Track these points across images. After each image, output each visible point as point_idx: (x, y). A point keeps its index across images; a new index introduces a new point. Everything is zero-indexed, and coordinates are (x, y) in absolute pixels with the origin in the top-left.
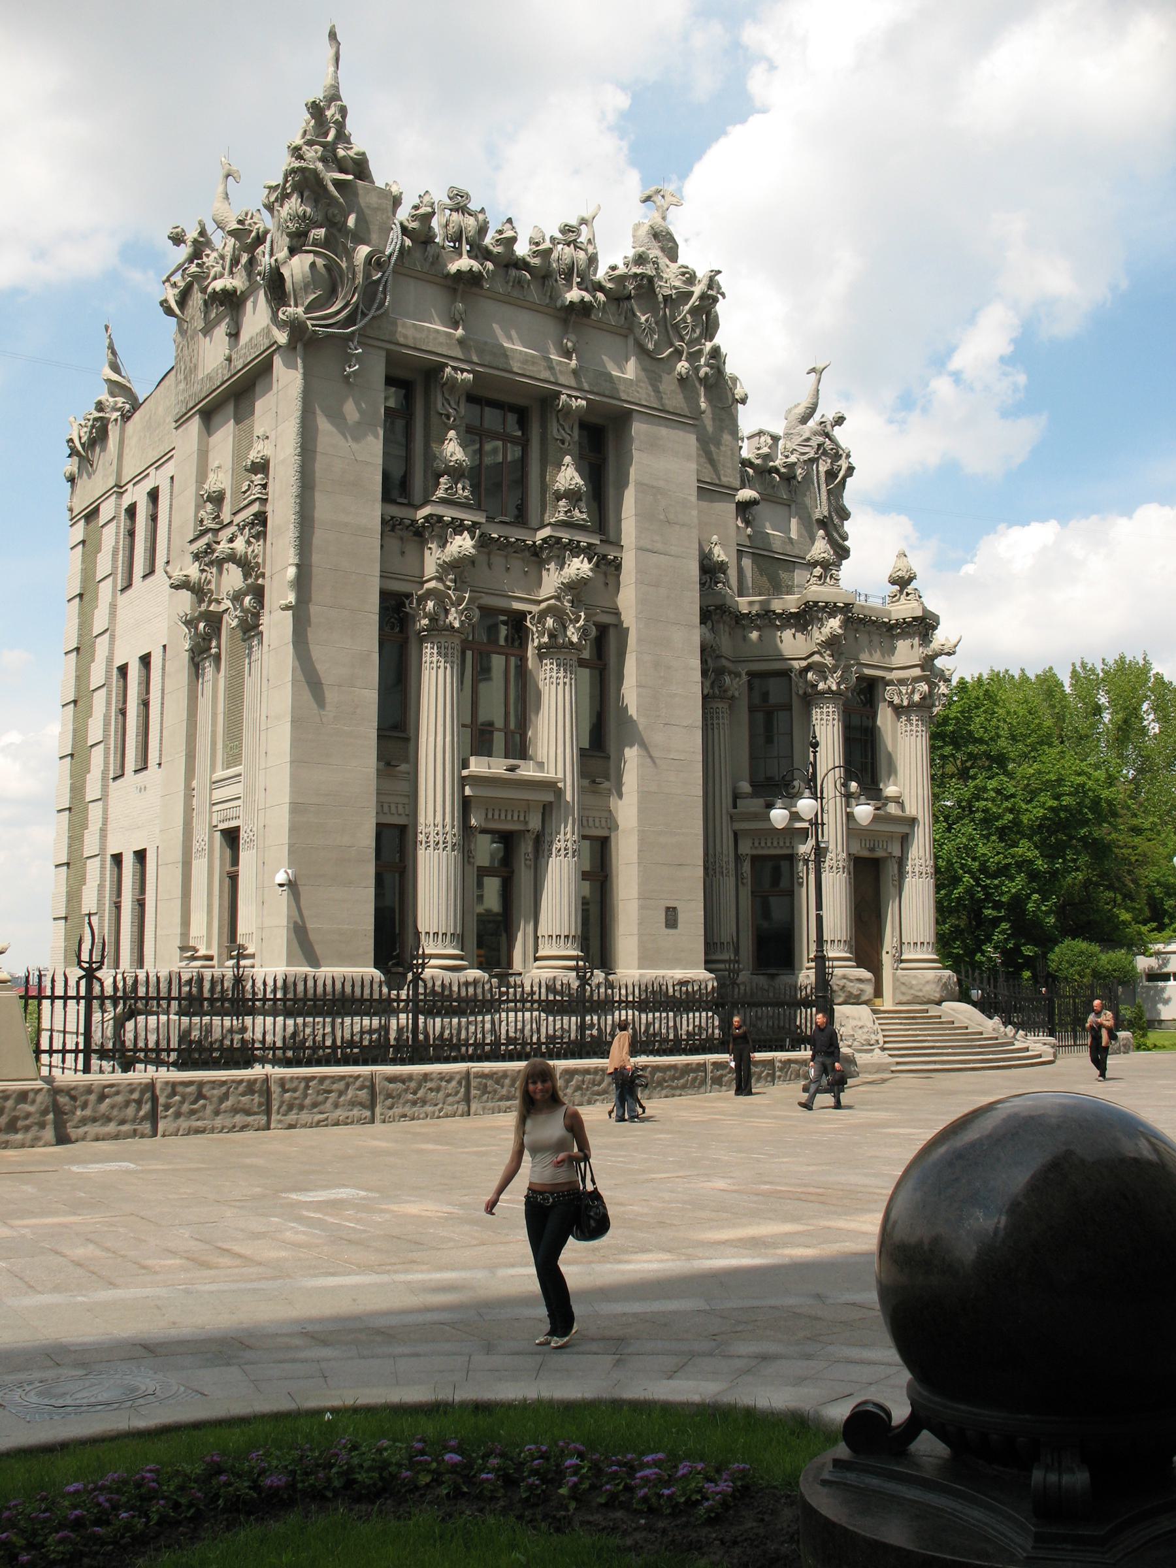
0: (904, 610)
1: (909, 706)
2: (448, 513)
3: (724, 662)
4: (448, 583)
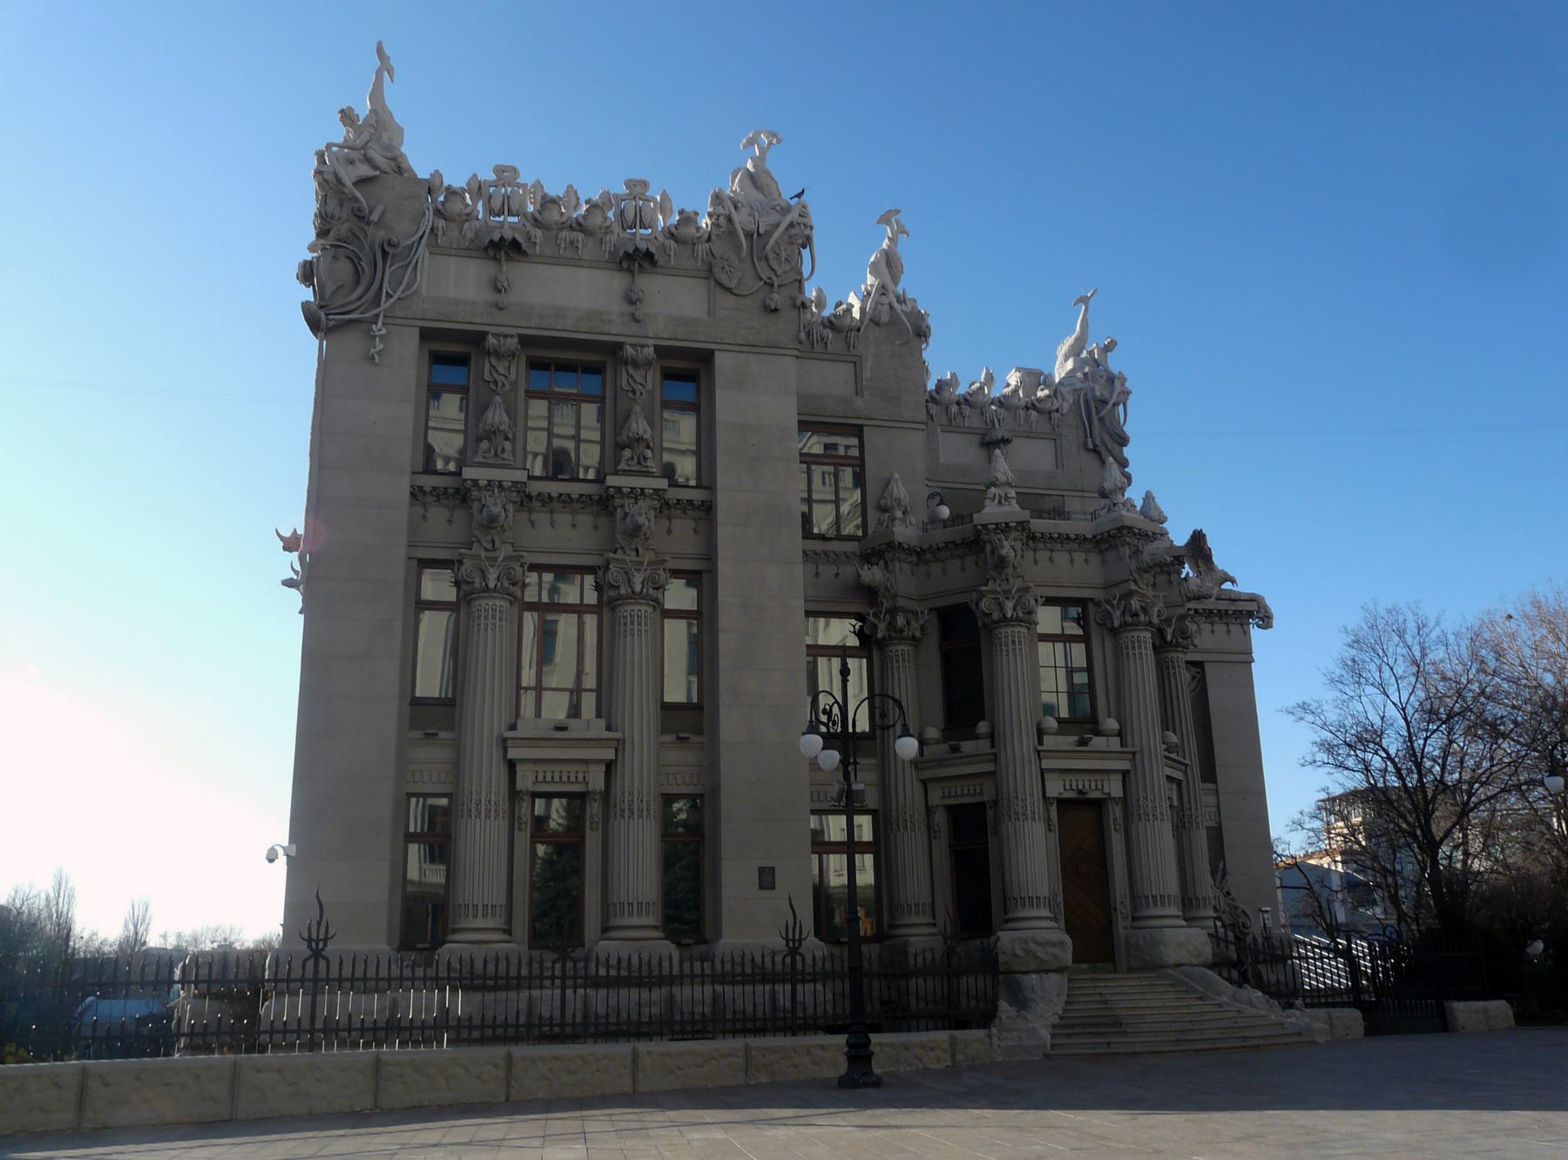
3: (901, 602)
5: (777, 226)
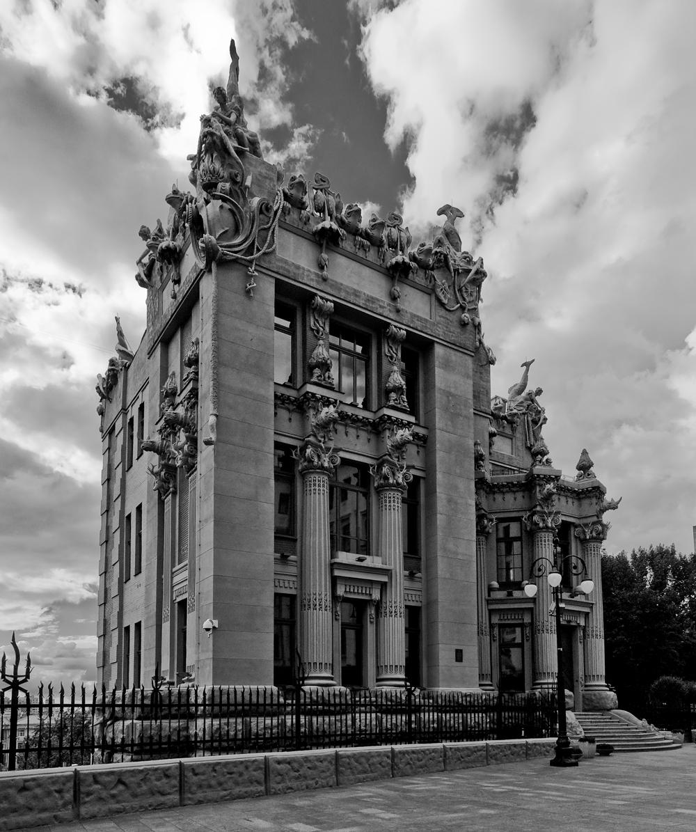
0: (586, 483)
2: (319, 392)
4: (320, 439)
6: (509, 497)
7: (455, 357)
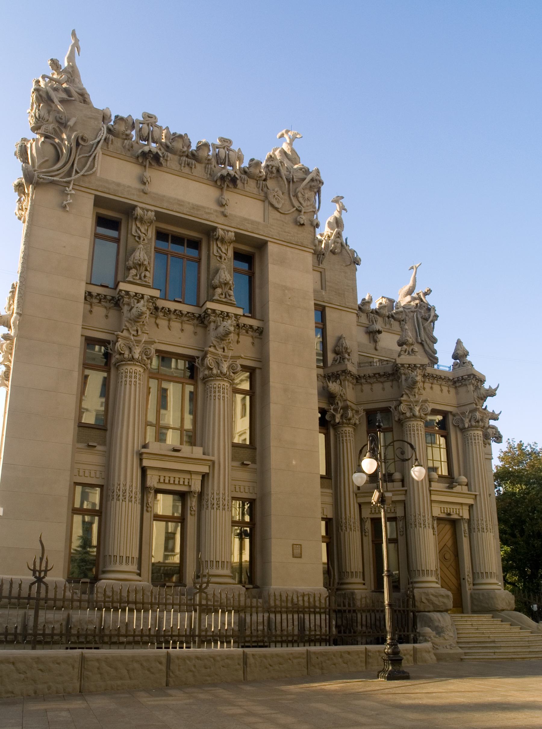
1: (468, 427)
5: (304, 179)
6: (377, 387)
7: (290, 253)
